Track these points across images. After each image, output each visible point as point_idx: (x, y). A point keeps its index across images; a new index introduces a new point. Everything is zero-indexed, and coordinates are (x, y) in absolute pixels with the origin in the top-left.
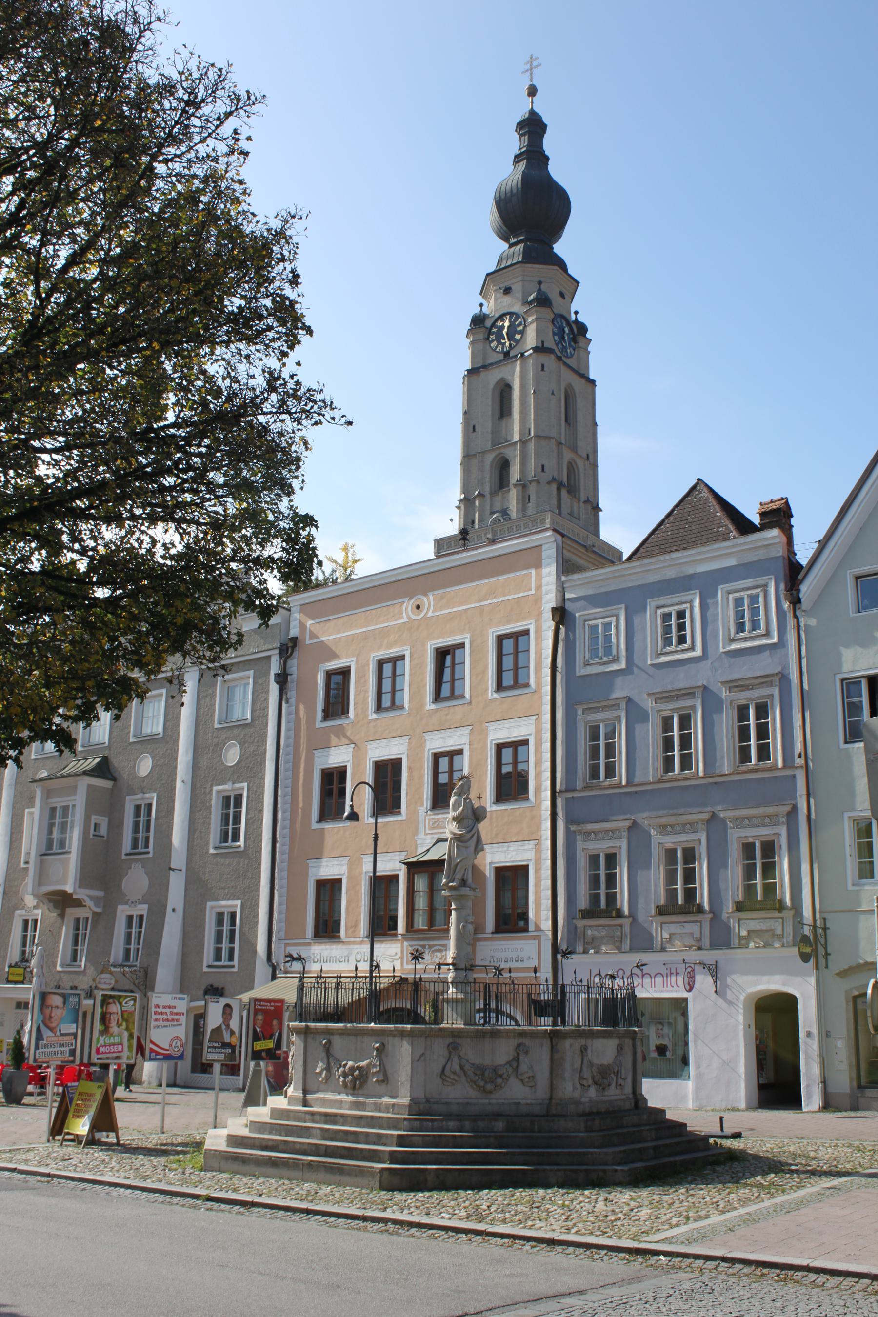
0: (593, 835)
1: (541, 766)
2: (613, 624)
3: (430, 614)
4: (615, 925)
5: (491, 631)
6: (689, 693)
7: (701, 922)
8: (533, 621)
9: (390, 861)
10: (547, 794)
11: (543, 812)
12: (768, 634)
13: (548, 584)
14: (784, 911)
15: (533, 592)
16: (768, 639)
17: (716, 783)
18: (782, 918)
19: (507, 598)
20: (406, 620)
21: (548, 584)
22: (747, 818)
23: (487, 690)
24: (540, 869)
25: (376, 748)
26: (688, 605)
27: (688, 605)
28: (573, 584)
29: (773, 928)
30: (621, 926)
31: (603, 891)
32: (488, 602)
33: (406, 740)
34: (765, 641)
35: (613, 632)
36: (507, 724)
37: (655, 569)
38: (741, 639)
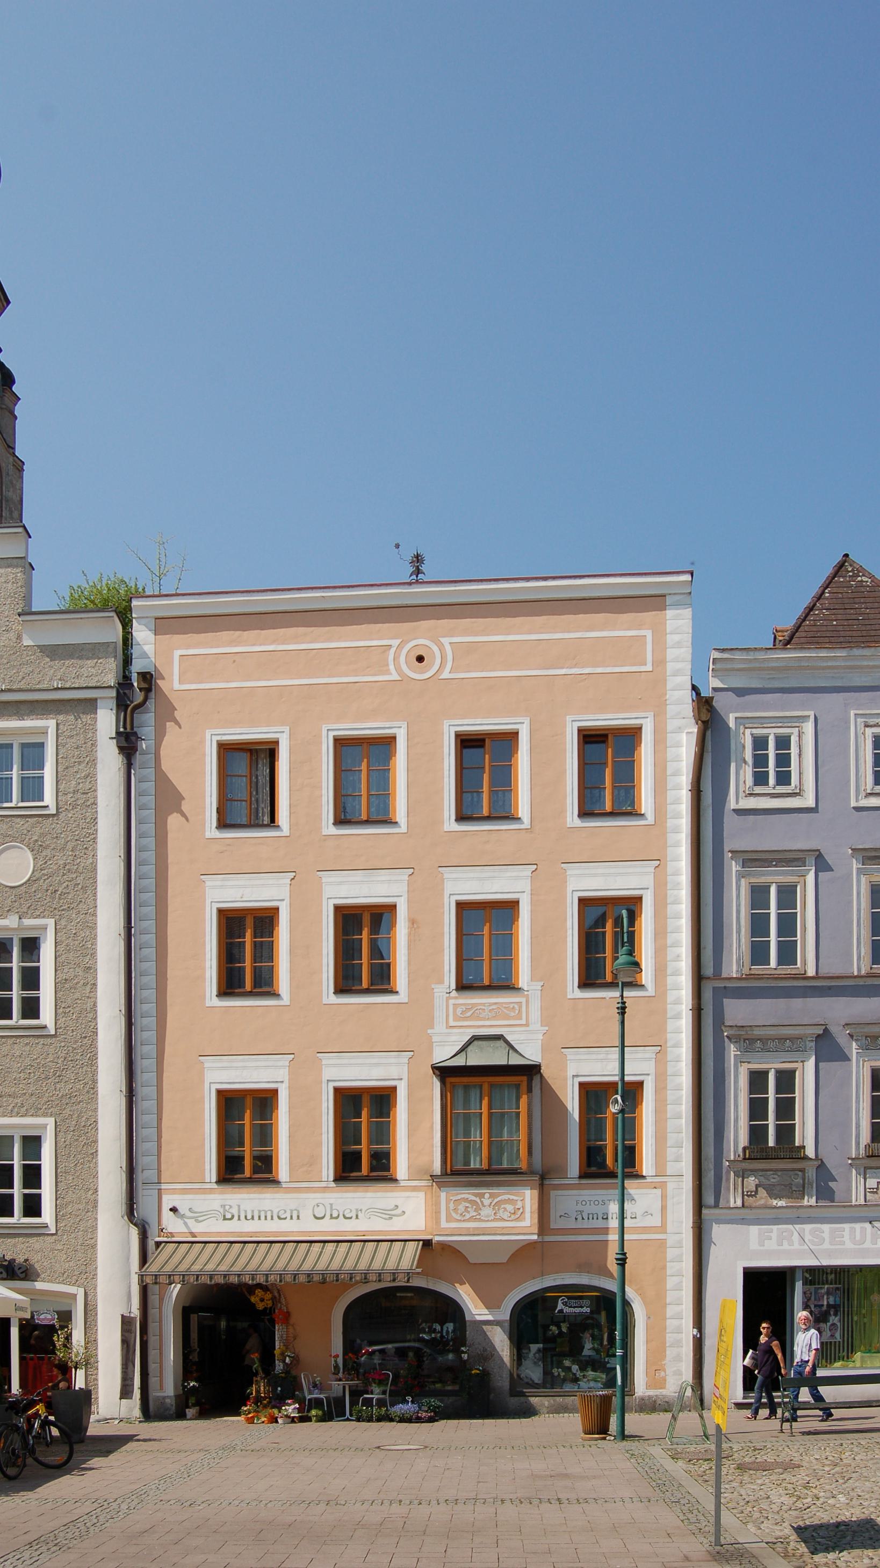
2: (794, 739)
8: (650, 715)
13: (676, 660)
21: (676, 660)
23: (563, 811)
24: (665, 1088)
28: (729, 666)
30: (803, 1170)
35: (794, 751)
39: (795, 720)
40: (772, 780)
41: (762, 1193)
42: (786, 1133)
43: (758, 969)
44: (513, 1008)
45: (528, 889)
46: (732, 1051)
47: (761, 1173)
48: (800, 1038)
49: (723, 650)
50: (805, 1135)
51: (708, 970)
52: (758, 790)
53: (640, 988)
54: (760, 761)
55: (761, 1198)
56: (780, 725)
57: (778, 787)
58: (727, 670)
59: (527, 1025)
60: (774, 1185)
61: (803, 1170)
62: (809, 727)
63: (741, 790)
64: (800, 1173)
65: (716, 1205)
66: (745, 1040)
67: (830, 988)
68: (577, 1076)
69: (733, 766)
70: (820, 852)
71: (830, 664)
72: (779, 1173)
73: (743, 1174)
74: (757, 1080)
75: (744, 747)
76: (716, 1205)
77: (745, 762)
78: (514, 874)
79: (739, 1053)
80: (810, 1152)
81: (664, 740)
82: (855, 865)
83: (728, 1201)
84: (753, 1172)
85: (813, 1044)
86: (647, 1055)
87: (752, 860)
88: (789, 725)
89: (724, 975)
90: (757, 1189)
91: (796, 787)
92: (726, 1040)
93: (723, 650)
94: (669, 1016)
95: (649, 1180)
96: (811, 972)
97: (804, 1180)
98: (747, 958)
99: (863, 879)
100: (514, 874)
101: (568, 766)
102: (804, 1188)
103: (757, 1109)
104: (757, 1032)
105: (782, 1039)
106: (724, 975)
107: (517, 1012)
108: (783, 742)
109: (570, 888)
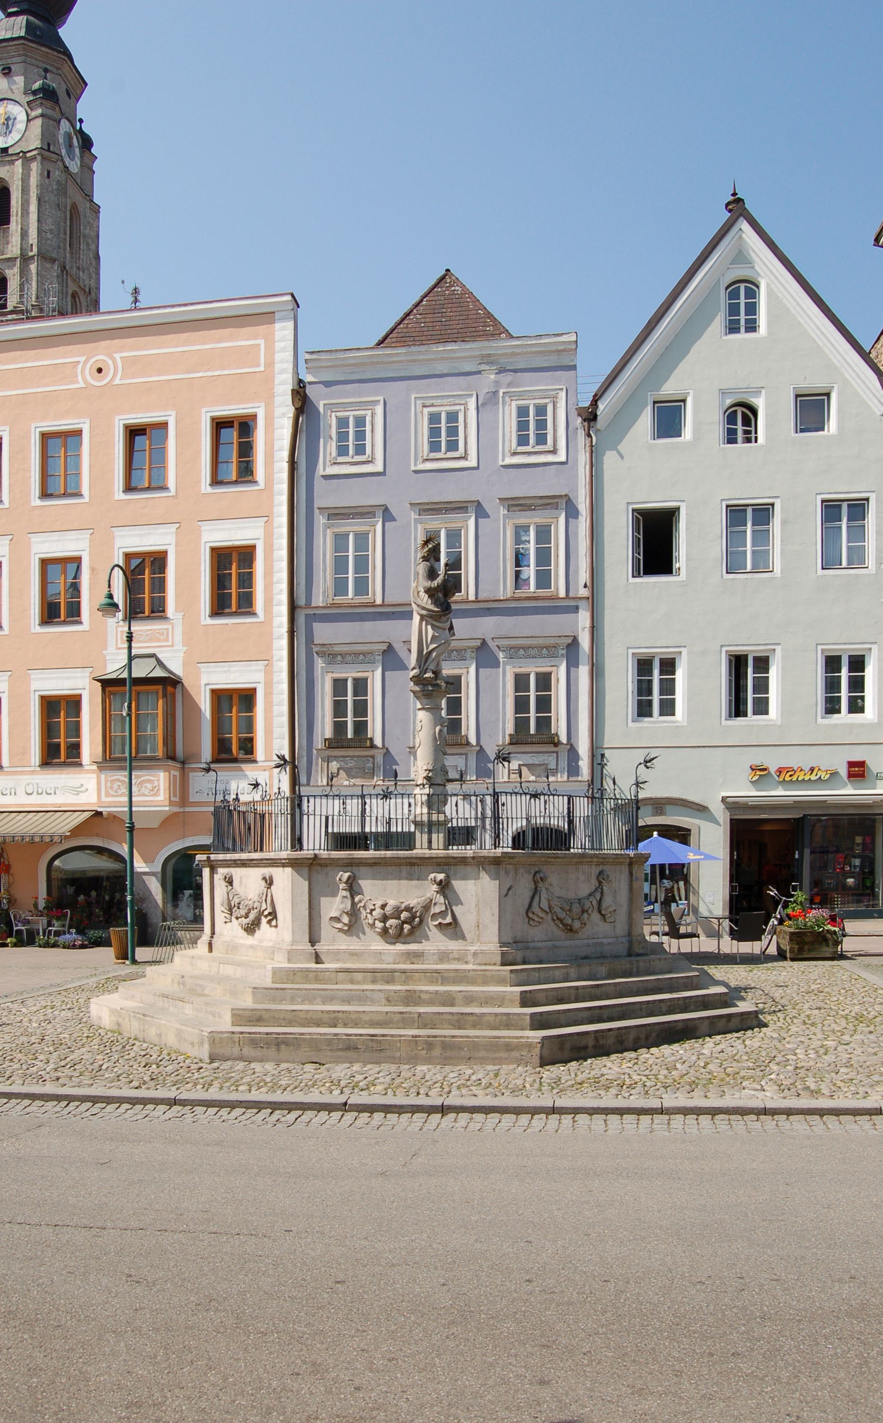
0: (339, 658)
1: (272, 576)
2: (368, 419)
3: (117, 381)
4: (366, 756)
5: (204, 410)
6: (460, 507)
7: (466, 755)
8: (263, 405)
9: (69, 678)
10: (283, 609)
11: (274, 630)
12: (554, 452)
13: (282, 362)
14: (560, 746)
15: (262, 369)
16: (554, 456)
17: (488, 609)
18: (557, 753)
19: (226, 372)
20: (82, 384)
21: (282, 362)
22: (523, 648)
23: (199, 482)
24: (272, 693)
25: (43, 542)
26: (462, 407)
27: (462, 407)
29: (546, 762)
30: (373, 757)
31: (350, 719)
32: (200, 375)
33: (86, 535)
34: (550, 458)
35: (368, 428)
36: (226, 524)
37: (419, 361)
38: (524, 453)
39: (370, 404)
40: (351, 451)
41: (342, 774)
42: (361, 727)
43: (339, 599)
45: (173, 541)
46: (319, 663)
47: (341, 759)
48: (371, 653)
49: (312, 353)
50: (375, 731)
51: (301, 601)
52: (341, 459)
53: (253, 616)
54: (342, 436)
55: (342, 779)
56: (357, 408)
57: (355, 457)
58: (317, 368)
59: (172, 646)
60: (351, 769)
61: (373, 757)
62: (379, 410)
63: (328, 459)
64: (371, 759)
65: (308, 784)
66: (329, 655)
67: (393, 613)
68: (208, 684)
69: (322, 441)
70: (387, 507)
71: (394, 359)
72: (355, 759)
73: (328, 760)
74: (339, 686)
75: (330, 426)
76: (308, 784)
77: (331, 438)
79: (324, 665)
80: (378, 742)
81: (272, 424)
82: (414, 516)
83: (317, 781)
84: (336, 758)
85: (380, 658)
86: (258, 668)
87: (336, 514)
88: (365, 408)
89: (313, 605)
90: (338, 771)
91: (369, 456)
92: (315, 654)
93: (312, 353)
94: (274, 637)
95: (260, 764)
96: (379, 601)
97: (374, 764)
98: (331, 592)
99: (419, 527)
101: (203, 447)
102: (374, 770)
103: (339, 708)
104: (336, 649)
105: (357, 654)
106: (313, 605)
108: (360, 422)
109: (203, 540)
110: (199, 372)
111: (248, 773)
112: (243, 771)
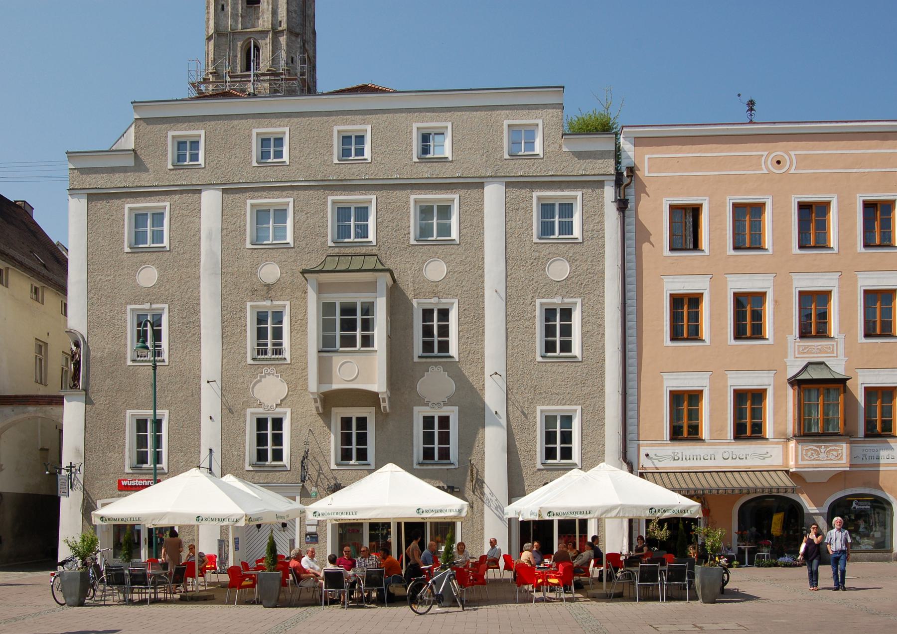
9: (757, 377)
19: (874, 170)
32: (855, 170)
33: (771, 277)
44: (830, 347)
45: (837, 285)
59: (837, 357)
68: (863, 384)
78: (830, 277)
100: (830, 277)
107: (831, 350)
109: (859, 285)
110: (854, 168)
111: (892, 444)
112: (888, 443)
